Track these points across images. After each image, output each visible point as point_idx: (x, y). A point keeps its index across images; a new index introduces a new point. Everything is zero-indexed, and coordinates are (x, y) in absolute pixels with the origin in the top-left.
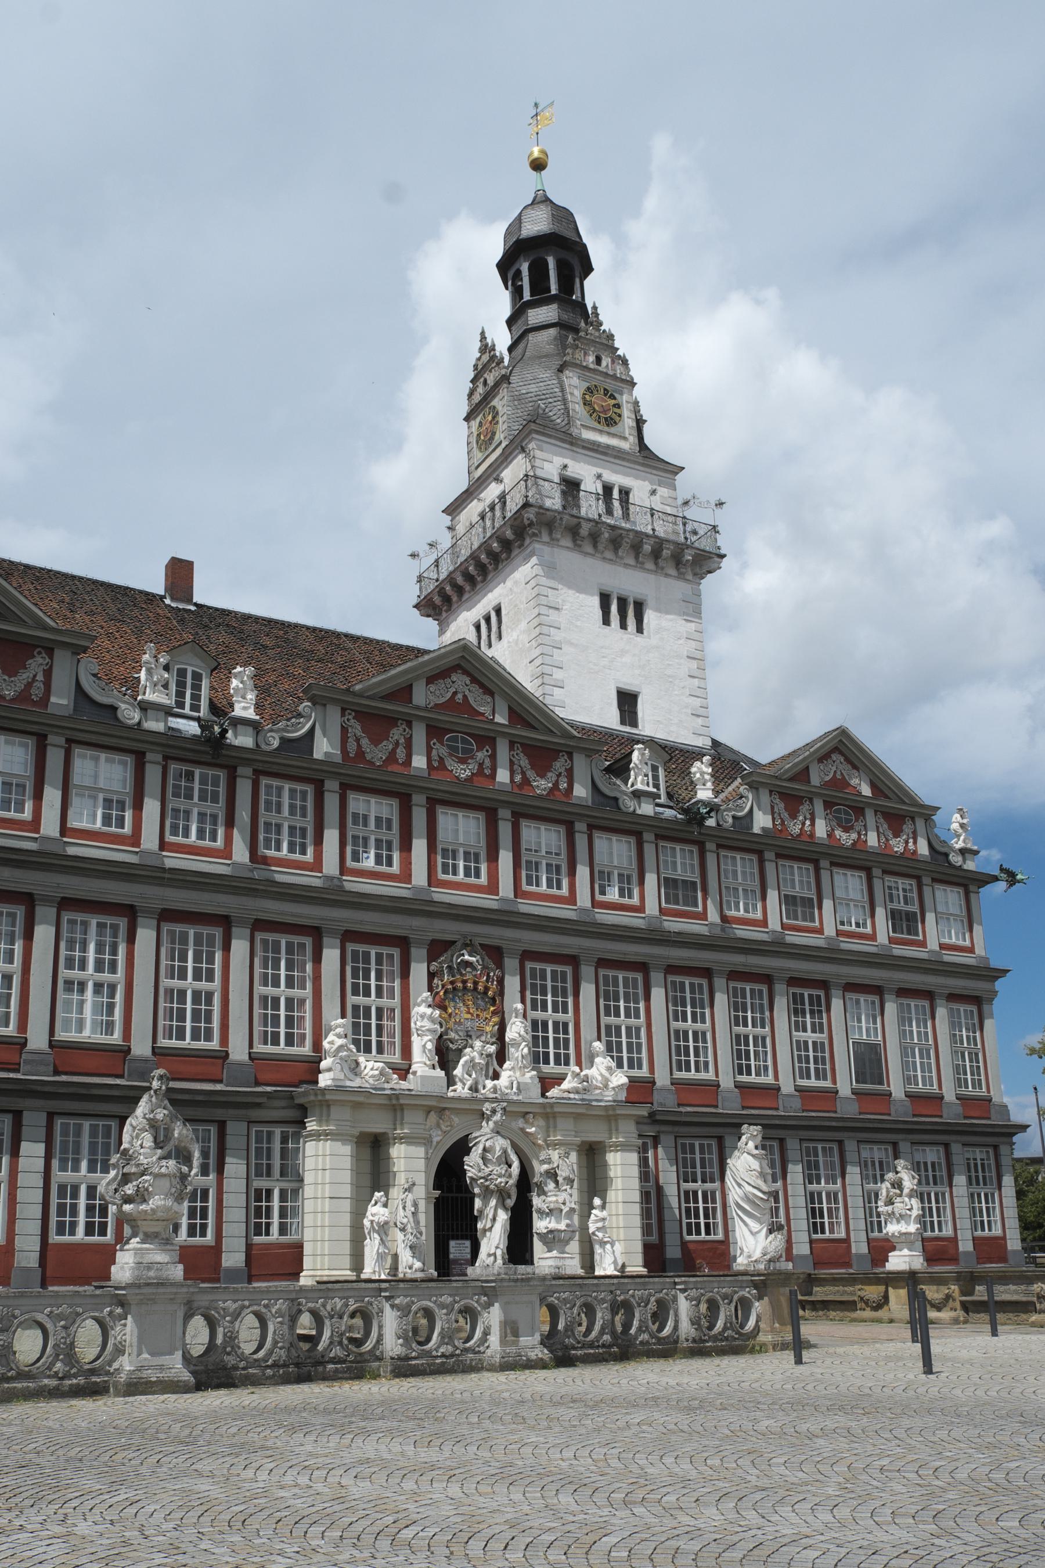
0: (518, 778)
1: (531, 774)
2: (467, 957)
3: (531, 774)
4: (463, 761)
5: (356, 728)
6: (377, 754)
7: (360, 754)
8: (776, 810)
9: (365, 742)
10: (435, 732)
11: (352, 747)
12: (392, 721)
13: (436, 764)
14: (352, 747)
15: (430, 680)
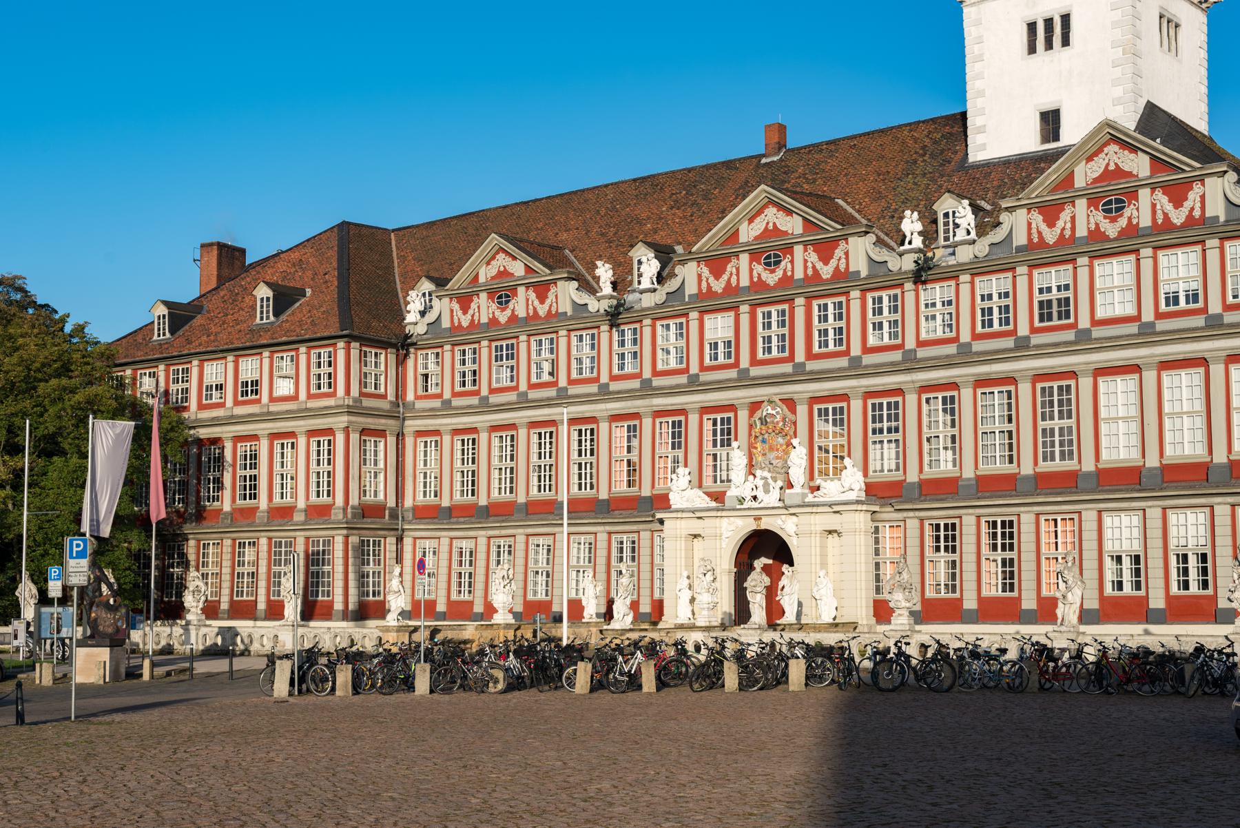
0: (810, 272)
1: (819, 265)
2: (770, 411)
3: (819, 265)
4: (773, 272)
5: (706, 272)
6: (718, 286)
7: (709, 287)
8: (1034, 226)
9: (711, 279)
10: (755, 256)
11: (704, 285)
12: (726, 258)
13: (755, 280)
14: (704, 285)
15: (751, 221)
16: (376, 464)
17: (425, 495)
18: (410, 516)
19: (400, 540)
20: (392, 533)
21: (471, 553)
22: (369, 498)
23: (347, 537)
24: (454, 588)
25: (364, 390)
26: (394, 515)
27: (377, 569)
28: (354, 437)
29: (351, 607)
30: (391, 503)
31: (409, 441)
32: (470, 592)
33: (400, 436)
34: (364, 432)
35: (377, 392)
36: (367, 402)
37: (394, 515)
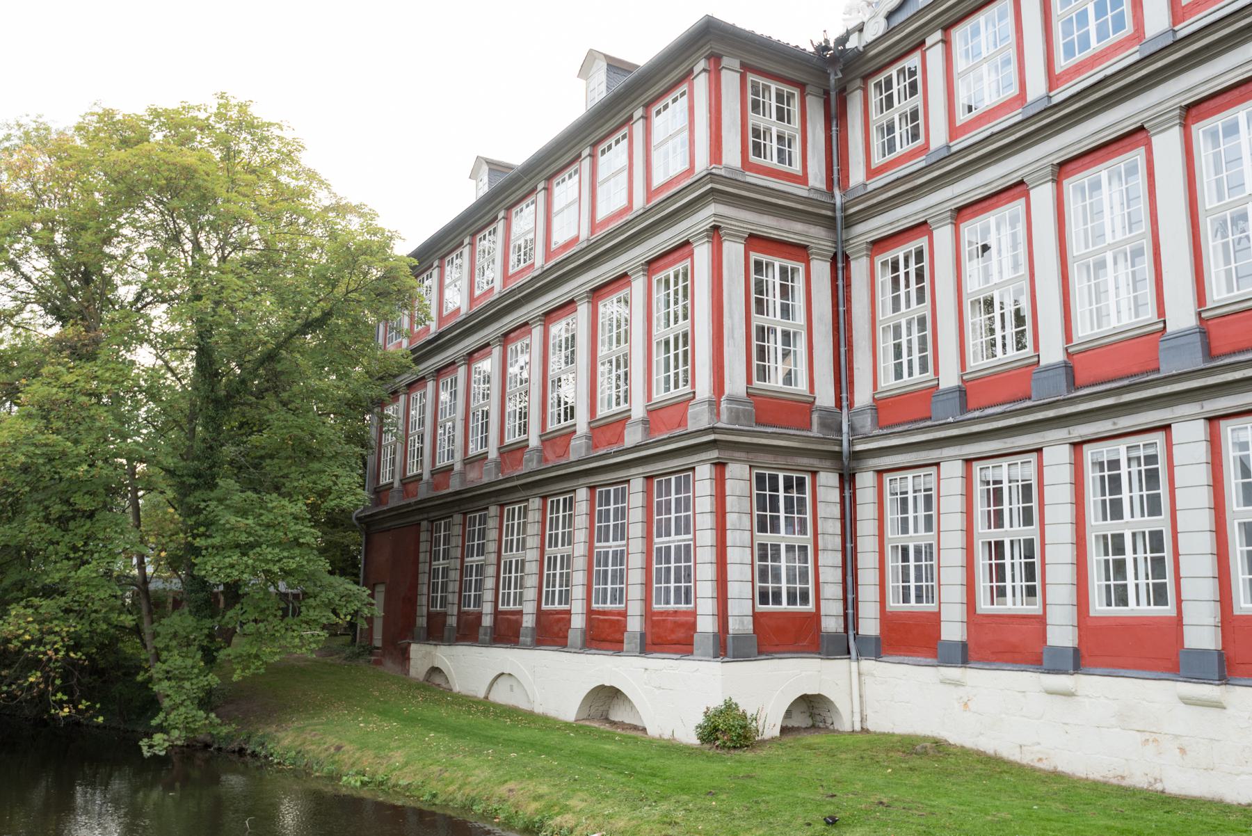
16: (786, 311)
17: (899, 375)
18: (866, 423)
19: (847, 480)
20: (828, 464)
21: (1027, 489)
22: (776, 382)
23: (720, 466)
24: (983, 584)
25: (753, 159)
26: (831, 422)
27: (797, 539)
28: (733, 251)
29: (734, 626)
30: (825, 396)
31: (859, 268)
32: (1031, 592)
33: (840, 263)
34: (754, 241)
35: (785, 167)
36: (752, 178)
37: (831, 422)
